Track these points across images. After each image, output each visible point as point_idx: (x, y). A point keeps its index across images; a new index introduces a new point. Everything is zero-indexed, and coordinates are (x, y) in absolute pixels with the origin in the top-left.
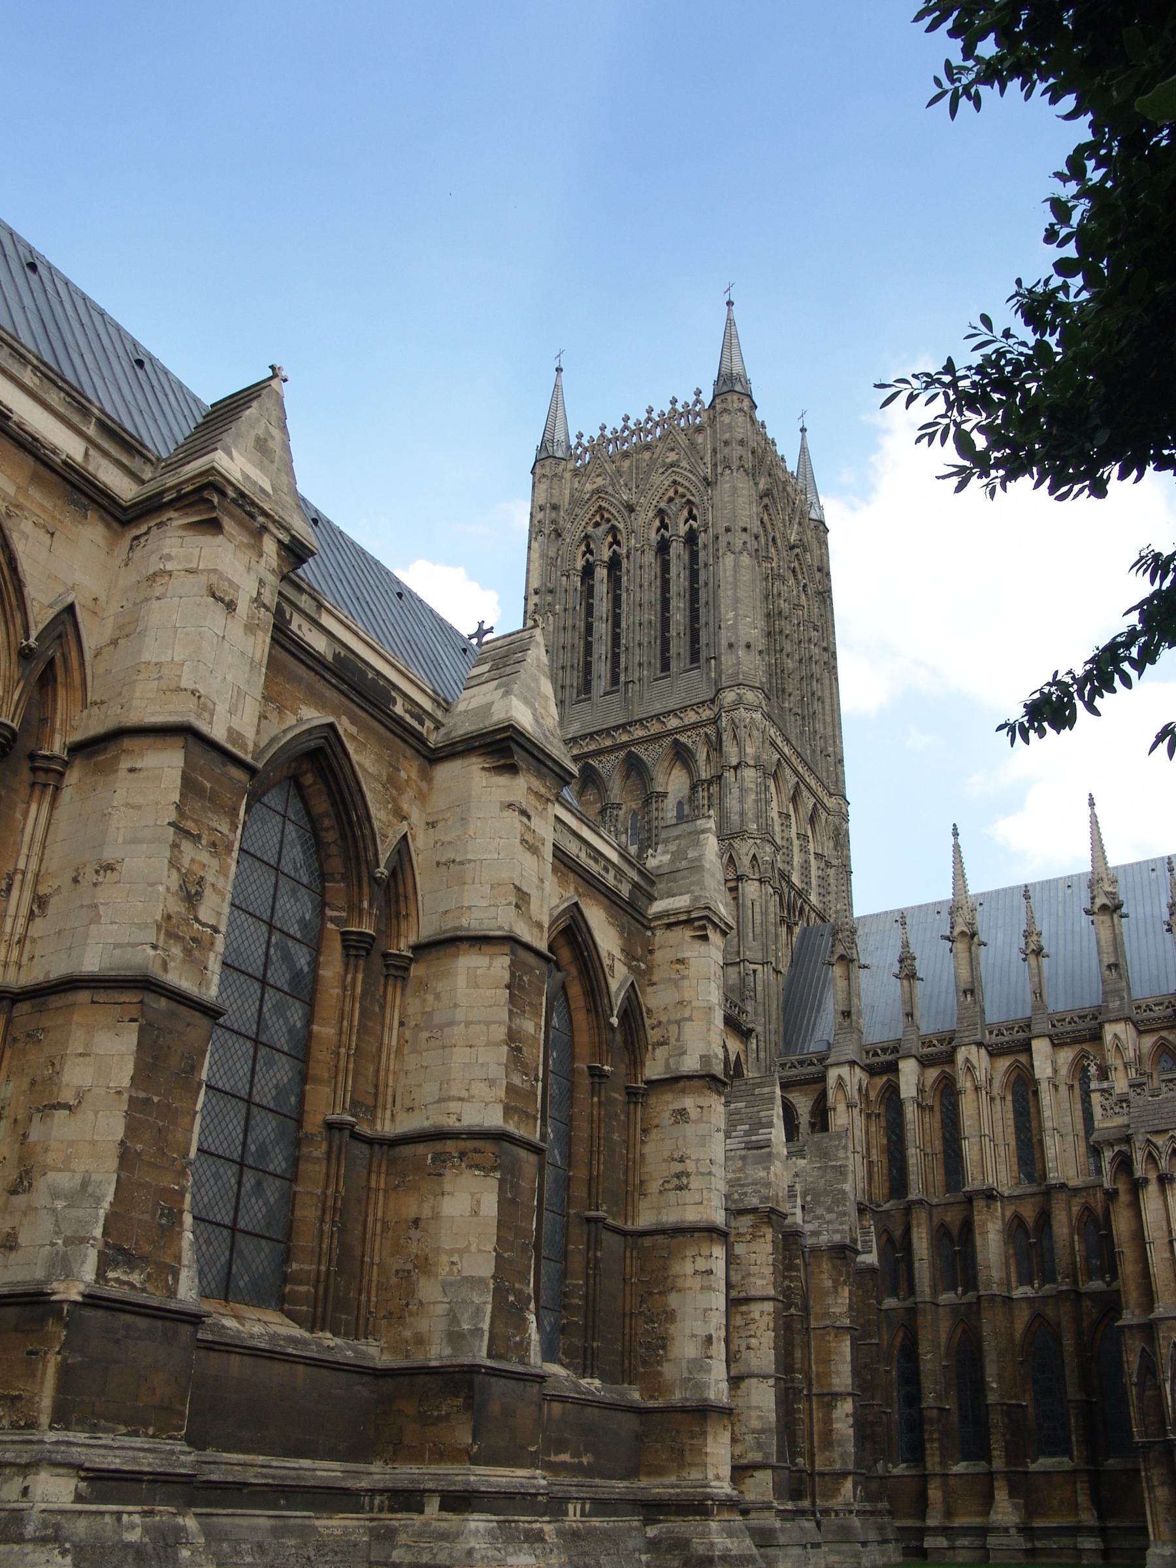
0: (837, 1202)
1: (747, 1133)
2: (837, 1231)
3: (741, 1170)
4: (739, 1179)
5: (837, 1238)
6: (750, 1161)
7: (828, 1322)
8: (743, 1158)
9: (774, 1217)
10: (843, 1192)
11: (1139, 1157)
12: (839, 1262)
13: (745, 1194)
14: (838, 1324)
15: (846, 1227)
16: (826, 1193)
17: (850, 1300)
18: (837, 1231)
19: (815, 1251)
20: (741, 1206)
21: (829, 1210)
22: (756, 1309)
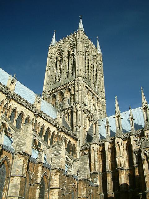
0: (85, 170)
1: (56, 152)
2: (84, 176)
3: (54, 160)
4: (54, 162)
5: (84, 178)
6: (56, 158)
7: (81, 196)
8: (55, 158)
9: (61, 170)
10: (86, 168)
11: (142, 154)
12: (84, 183)
13: (54, 165)
14: (84, 196)
15: (86, 175)
16: (83, 168)
17: (87, 191)
18: (84, 176)
19: (79, 180)
20: (53, 168)
21: (83, 172)
22: (55, 191)
